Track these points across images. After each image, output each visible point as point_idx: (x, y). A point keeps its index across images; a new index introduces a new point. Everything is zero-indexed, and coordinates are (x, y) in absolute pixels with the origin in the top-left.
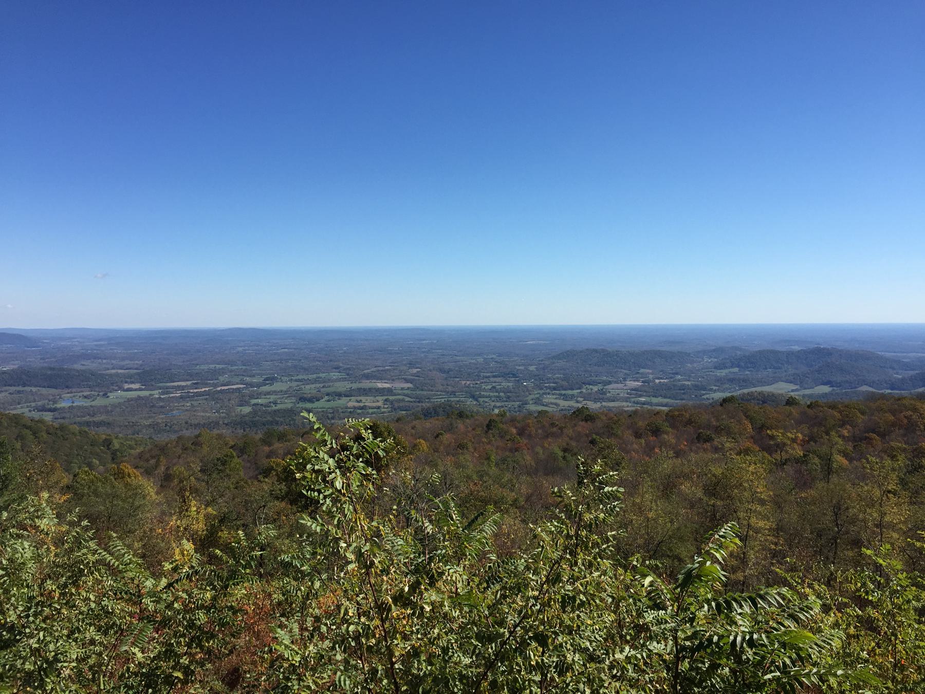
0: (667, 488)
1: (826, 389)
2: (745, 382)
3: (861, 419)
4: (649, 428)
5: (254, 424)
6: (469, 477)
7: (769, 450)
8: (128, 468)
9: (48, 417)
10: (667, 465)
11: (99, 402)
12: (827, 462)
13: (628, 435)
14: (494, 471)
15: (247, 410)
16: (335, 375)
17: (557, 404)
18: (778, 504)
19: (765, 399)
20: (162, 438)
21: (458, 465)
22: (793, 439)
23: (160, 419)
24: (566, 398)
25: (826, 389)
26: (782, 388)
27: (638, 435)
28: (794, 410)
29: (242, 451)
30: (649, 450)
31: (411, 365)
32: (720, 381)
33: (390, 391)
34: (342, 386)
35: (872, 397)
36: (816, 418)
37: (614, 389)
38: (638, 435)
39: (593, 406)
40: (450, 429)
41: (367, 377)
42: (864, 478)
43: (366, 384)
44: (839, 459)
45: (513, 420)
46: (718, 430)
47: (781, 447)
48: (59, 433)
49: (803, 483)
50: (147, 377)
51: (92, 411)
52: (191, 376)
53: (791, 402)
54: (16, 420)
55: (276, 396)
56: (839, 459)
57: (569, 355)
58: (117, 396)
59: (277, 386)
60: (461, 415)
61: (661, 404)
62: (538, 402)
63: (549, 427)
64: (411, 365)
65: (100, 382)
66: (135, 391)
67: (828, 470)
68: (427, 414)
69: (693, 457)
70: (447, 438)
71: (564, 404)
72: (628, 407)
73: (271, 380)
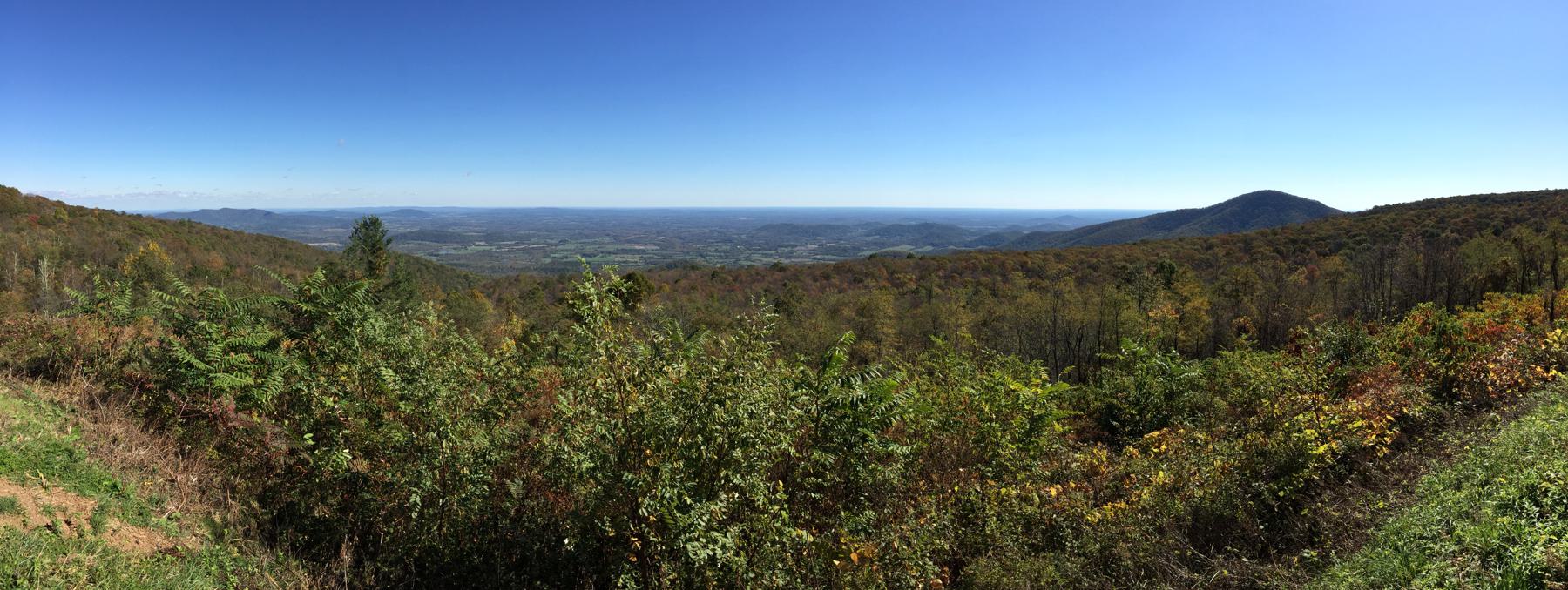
0: (834, 312)
1: (930, 248)
2: (883, 245)
3: (949, 266)
4: (823, 275)
5: (553, 270)
6: (698, 309)
7: (897, 286)
8: (477, 293)
9: (434, 259)
10: (833, 298)
11: (462, 252)
12: (930, 291)
13: (809, 281)
14: (716, 305)
15: (548, 261)
16: (607, 240)
17: (761, 260)
18: (900, 318)
19: (895, 255)
20: (497, 276)
21: (690, 300)
22: (910, 279)
23: (496, 264)
24: (767, 256)
25: (930, 248)
26: (905, 248)
27: (815, 280)
28: (911, 261)
29: (545, 287)
30: (822, 289)
31: (659, 234)
32: (868, 244)
33: (644, 251)
34: (611, 248)
35: (955, 252)
36: (924, 266)
37: (799, 250)
38: (815, 280)
39: (785, 261)
40: (686, 276)
41: (629, 242)
42: (949, 300)
43: (627, 246)
44: (936, 290)
45: (730, 271)
46: (867, 275)
47: (903, 284)
48: (440, 269)
49: (916, 306)
50: (489, 238)
51: (460, 257)
52: (514, 238)
53: (910, 256)
54: (417, 260)
55: (569, 252)
56: (936, 290)
57: (768, 227)
58: (472, 249)
59: (568, 246)
60: (693, 268)
61: (831, 259)
62: (748, 259)
63: (755, 275)
64: (659, 234)
65: (462, 240)
66: (482, 246)
67: (930, 295)
68: (670, 267)
69: (850, 292)
70: (683, 283)
71: (765, 260)
72: (809, 262)
73: (563, 242)
